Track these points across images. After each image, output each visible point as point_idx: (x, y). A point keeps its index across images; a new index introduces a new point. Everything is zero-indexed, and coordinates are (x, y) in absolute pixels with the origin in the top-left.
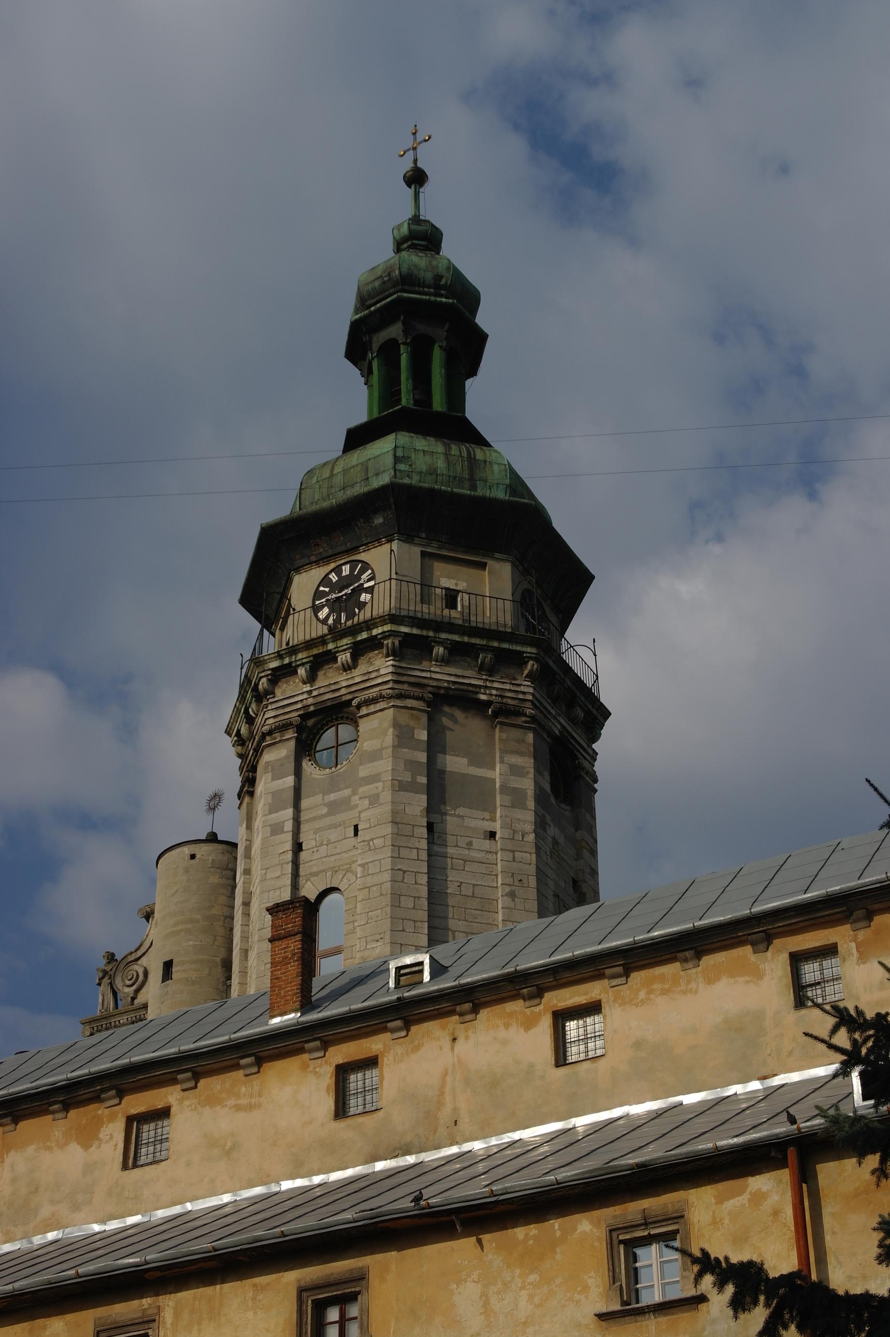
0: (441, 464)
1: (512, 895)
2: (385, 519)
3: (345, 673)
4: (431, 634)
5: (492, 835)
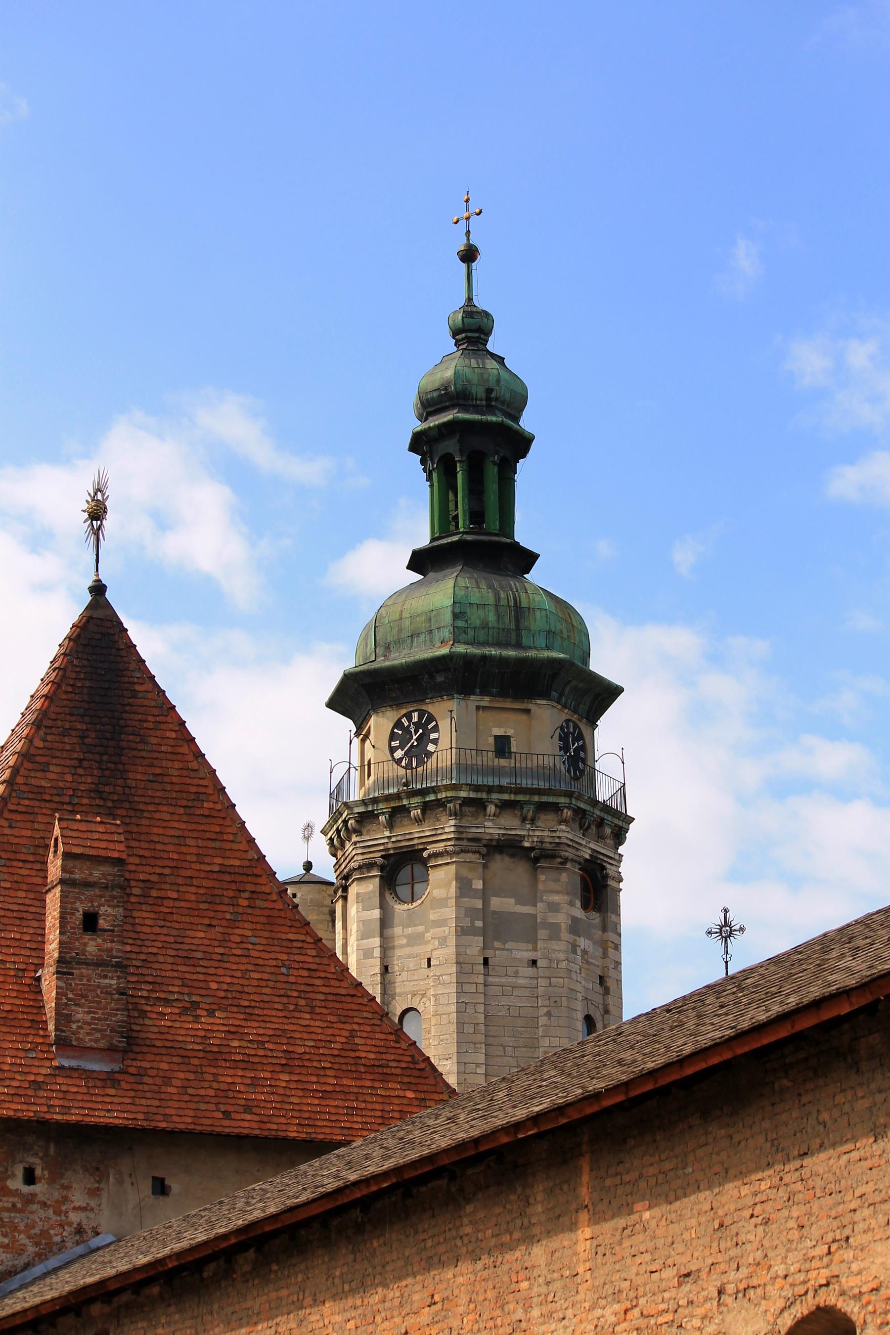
0: (492, 617)
1: (549, 1014)
5: (534, 962)
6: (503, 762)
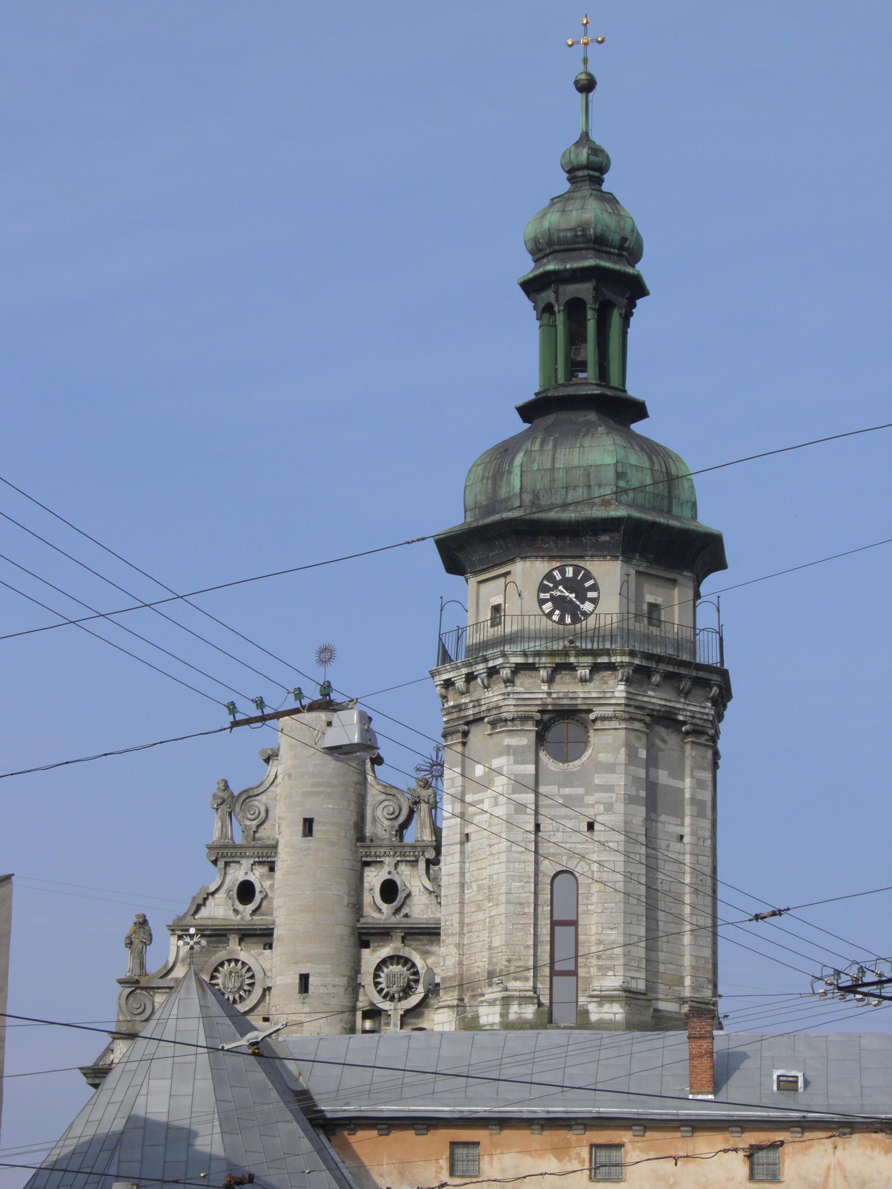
2: (611, 538)
3: (580, 684)
4: (654, 666)
6: (655, 631)
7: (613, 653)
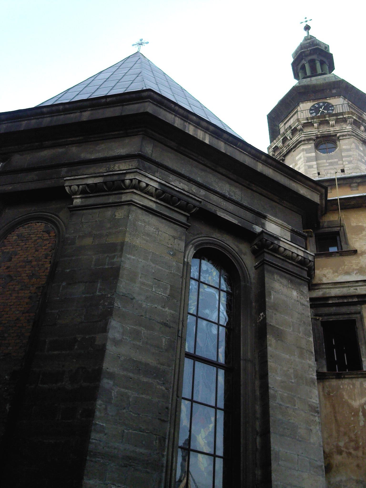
7: (344, 114)
